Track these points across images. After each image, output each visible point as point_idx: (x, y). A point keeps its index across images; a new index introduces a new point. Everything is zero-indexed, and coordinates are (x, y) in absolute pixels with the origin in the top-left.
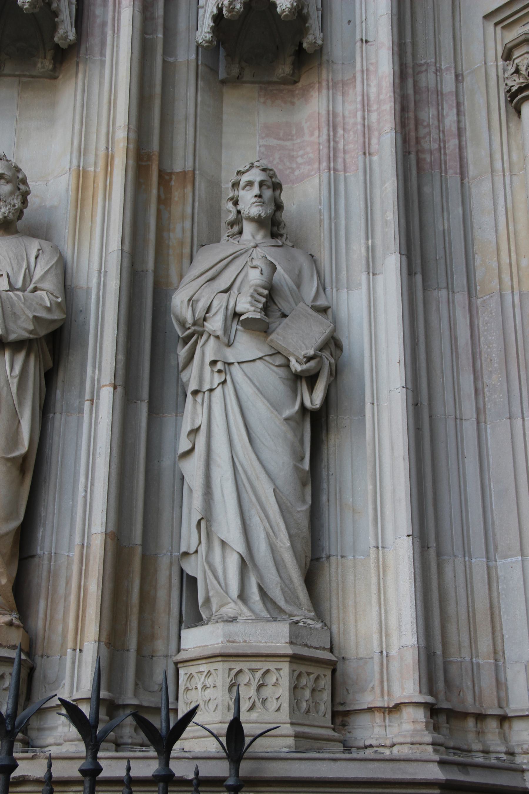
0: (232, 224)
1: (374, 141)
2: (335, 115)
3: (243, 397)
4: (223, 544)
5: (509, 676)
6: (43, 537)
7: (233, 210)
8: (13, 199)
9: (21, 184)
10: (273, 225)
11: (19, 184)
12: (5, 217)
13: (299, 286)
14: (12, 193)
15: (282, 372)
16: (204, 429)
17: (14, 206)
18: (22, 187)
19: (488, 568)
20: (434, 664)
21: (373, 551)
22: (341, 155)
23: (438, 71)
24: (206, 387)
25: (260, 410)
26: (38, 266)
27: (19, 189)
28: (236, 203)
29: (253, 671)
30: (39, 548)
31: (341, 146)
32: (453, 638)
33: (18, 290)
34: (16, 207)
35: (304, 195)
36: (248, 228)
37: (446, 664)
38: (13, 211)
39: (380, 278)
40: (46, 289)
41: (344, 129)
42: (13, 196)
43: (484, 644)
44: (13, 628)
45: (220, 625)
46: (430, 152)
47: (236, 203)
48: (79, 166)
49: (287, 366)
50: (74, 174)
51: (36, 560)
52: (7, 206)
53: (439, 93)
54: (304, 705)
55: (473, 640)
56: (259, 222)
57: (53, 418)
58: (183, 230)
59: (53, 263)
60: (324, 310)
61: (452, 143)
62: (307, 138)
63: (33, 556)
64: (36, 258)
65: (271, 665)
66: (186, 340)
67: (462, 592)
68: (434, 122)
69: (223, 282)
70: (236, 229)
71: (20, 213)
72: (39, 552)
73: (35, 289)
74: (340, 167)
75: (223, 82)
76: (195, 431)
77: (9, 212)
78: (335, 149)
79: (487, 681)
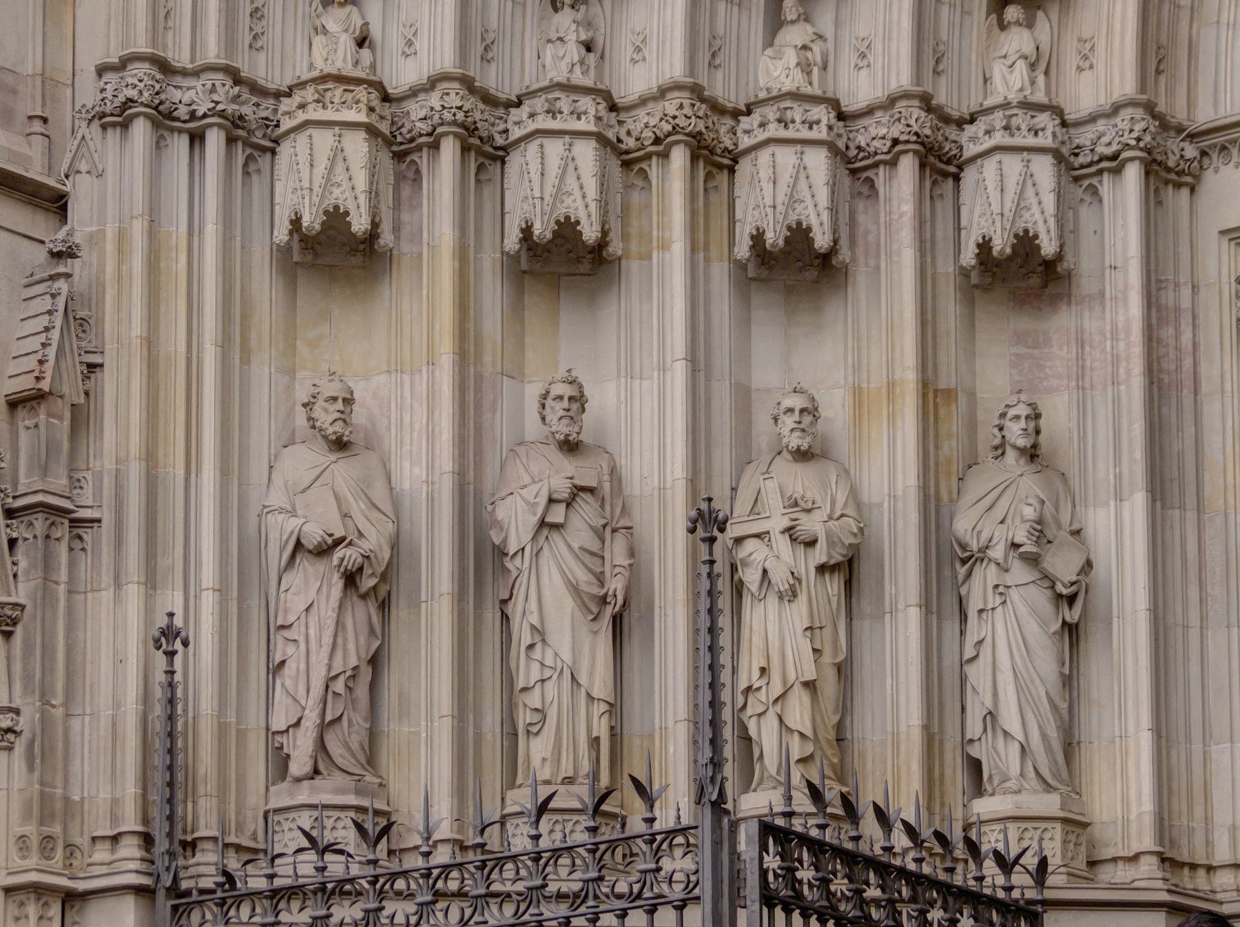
0: (996, 448)
1: (1122, 371)
2: (1083, 331)
3: (1019, 614)
4: (1006, 733)
5: (1216, 836)
7: (999, 436)
10: (1032, 454)
13: (1057, 510)
15: (1049, 593)
16: (989, 640)
19: (1205, 753)
20: (1163, 824)
21: (1117, 739)
22: (1088, 373)
23: (1177, 285)
24: (990, 606)
25: (1032, 627)
28: (1001, 429)
29: (1036, 829)
31: (1088, 363)
32: (1175, 806)
35: (1059, 415)
36: (1011, 455)
37: (1171, 826)
39: (1126, 504)
41: (1091, 346)
43: (1199, 812)
45: (1009, 796)
46: (1169, 373)
47: (1001, 429)
49: (1053, 587)
50: (851, 392)
53: (1177, 310)
54: (1070, 854)
55: (1190, 808)
56: (1022, 451)
58: (950, 447)
60: (1077, 533)
61: (1188, 362)
62: (1055, 350)
65: (1049, 825)
66: (964, 562)
67: (1183, 771)
68: (1172, 342)
69: (999, 512)
70: (1000, 452)
74: (1087, 385)
75: (975, 286)
76: (980, 642)
78: (1083, 367)
79: (1199, 839)
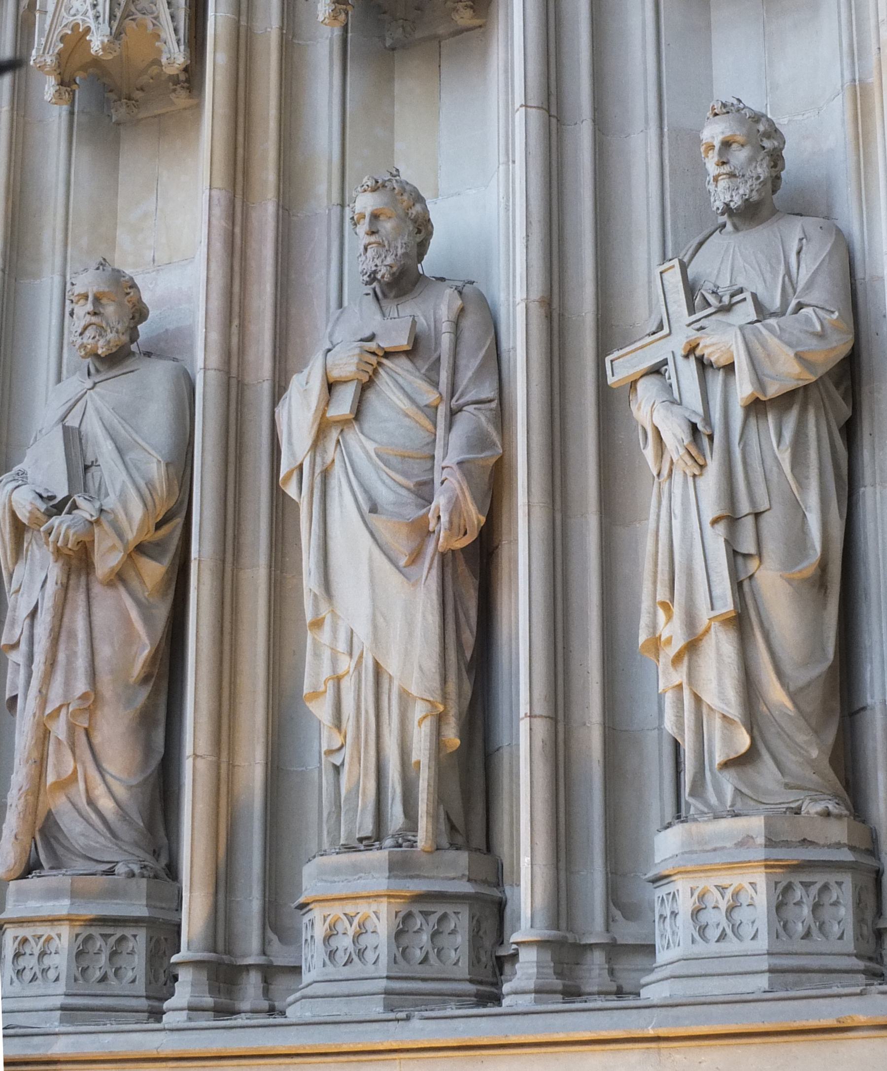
6: (872, 678)
8: (756, 167)
9: (764, 139)
11: (762, 141)
12: (747, 200)
14: (751, 159)
17: (758, 178)
18: (767, 144)
26: (803, 265)
27: (764, 148)
30: (868, 696)
33: (773, 314)
34: (762, 179)
38: (758, 187)
40: (813, 302)
42: (754, 164)
44: (832, 820)
48: (854, 80)
50: (848, 94)
51: (868, 712)
52: (746, 182)
57: (864, 492)
59: (824, 255)
63: (864, 709)
64: (799, 253)
71: (775, 181)
72: (869, 701)
73: (800, 306)
77: (752, 191)
